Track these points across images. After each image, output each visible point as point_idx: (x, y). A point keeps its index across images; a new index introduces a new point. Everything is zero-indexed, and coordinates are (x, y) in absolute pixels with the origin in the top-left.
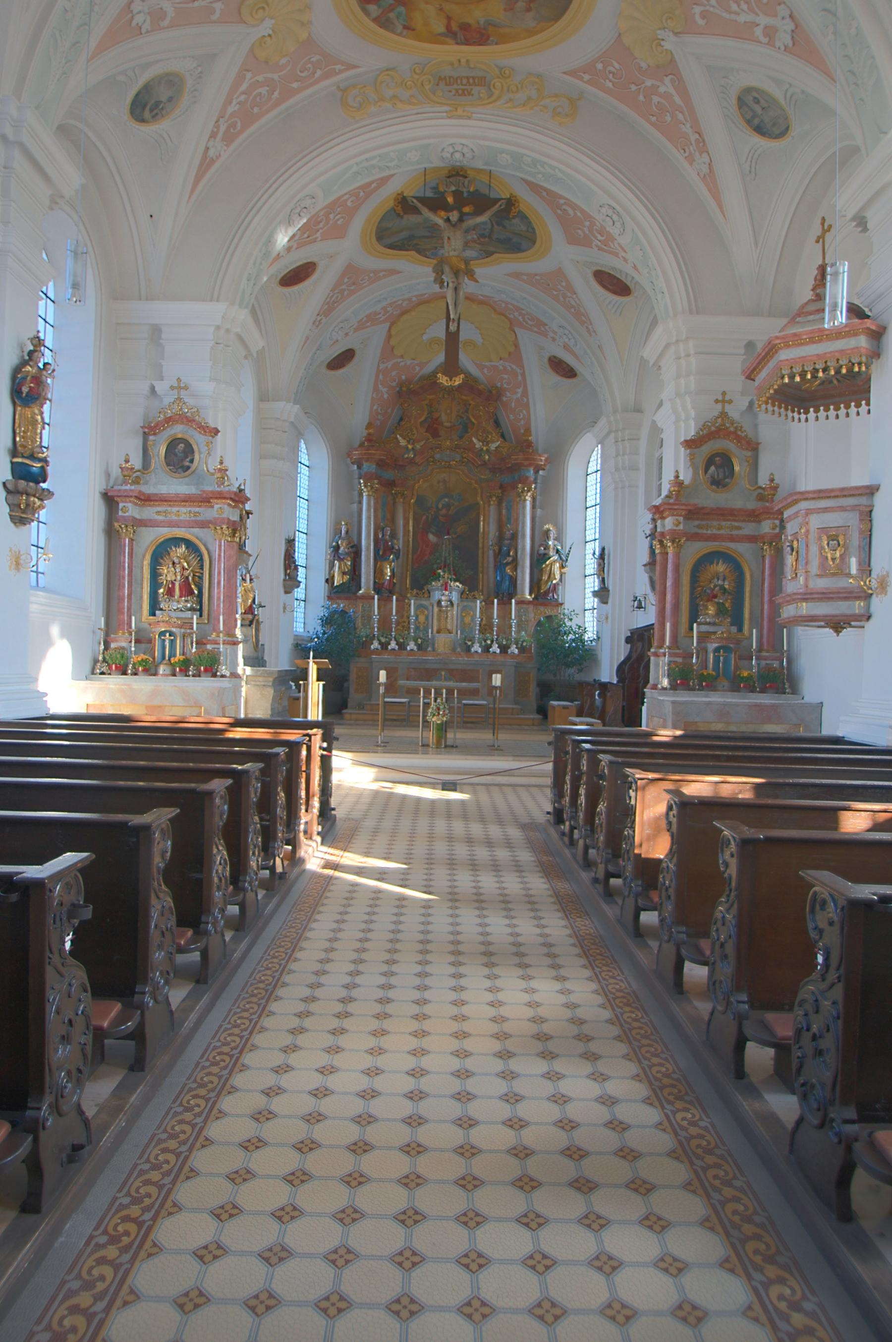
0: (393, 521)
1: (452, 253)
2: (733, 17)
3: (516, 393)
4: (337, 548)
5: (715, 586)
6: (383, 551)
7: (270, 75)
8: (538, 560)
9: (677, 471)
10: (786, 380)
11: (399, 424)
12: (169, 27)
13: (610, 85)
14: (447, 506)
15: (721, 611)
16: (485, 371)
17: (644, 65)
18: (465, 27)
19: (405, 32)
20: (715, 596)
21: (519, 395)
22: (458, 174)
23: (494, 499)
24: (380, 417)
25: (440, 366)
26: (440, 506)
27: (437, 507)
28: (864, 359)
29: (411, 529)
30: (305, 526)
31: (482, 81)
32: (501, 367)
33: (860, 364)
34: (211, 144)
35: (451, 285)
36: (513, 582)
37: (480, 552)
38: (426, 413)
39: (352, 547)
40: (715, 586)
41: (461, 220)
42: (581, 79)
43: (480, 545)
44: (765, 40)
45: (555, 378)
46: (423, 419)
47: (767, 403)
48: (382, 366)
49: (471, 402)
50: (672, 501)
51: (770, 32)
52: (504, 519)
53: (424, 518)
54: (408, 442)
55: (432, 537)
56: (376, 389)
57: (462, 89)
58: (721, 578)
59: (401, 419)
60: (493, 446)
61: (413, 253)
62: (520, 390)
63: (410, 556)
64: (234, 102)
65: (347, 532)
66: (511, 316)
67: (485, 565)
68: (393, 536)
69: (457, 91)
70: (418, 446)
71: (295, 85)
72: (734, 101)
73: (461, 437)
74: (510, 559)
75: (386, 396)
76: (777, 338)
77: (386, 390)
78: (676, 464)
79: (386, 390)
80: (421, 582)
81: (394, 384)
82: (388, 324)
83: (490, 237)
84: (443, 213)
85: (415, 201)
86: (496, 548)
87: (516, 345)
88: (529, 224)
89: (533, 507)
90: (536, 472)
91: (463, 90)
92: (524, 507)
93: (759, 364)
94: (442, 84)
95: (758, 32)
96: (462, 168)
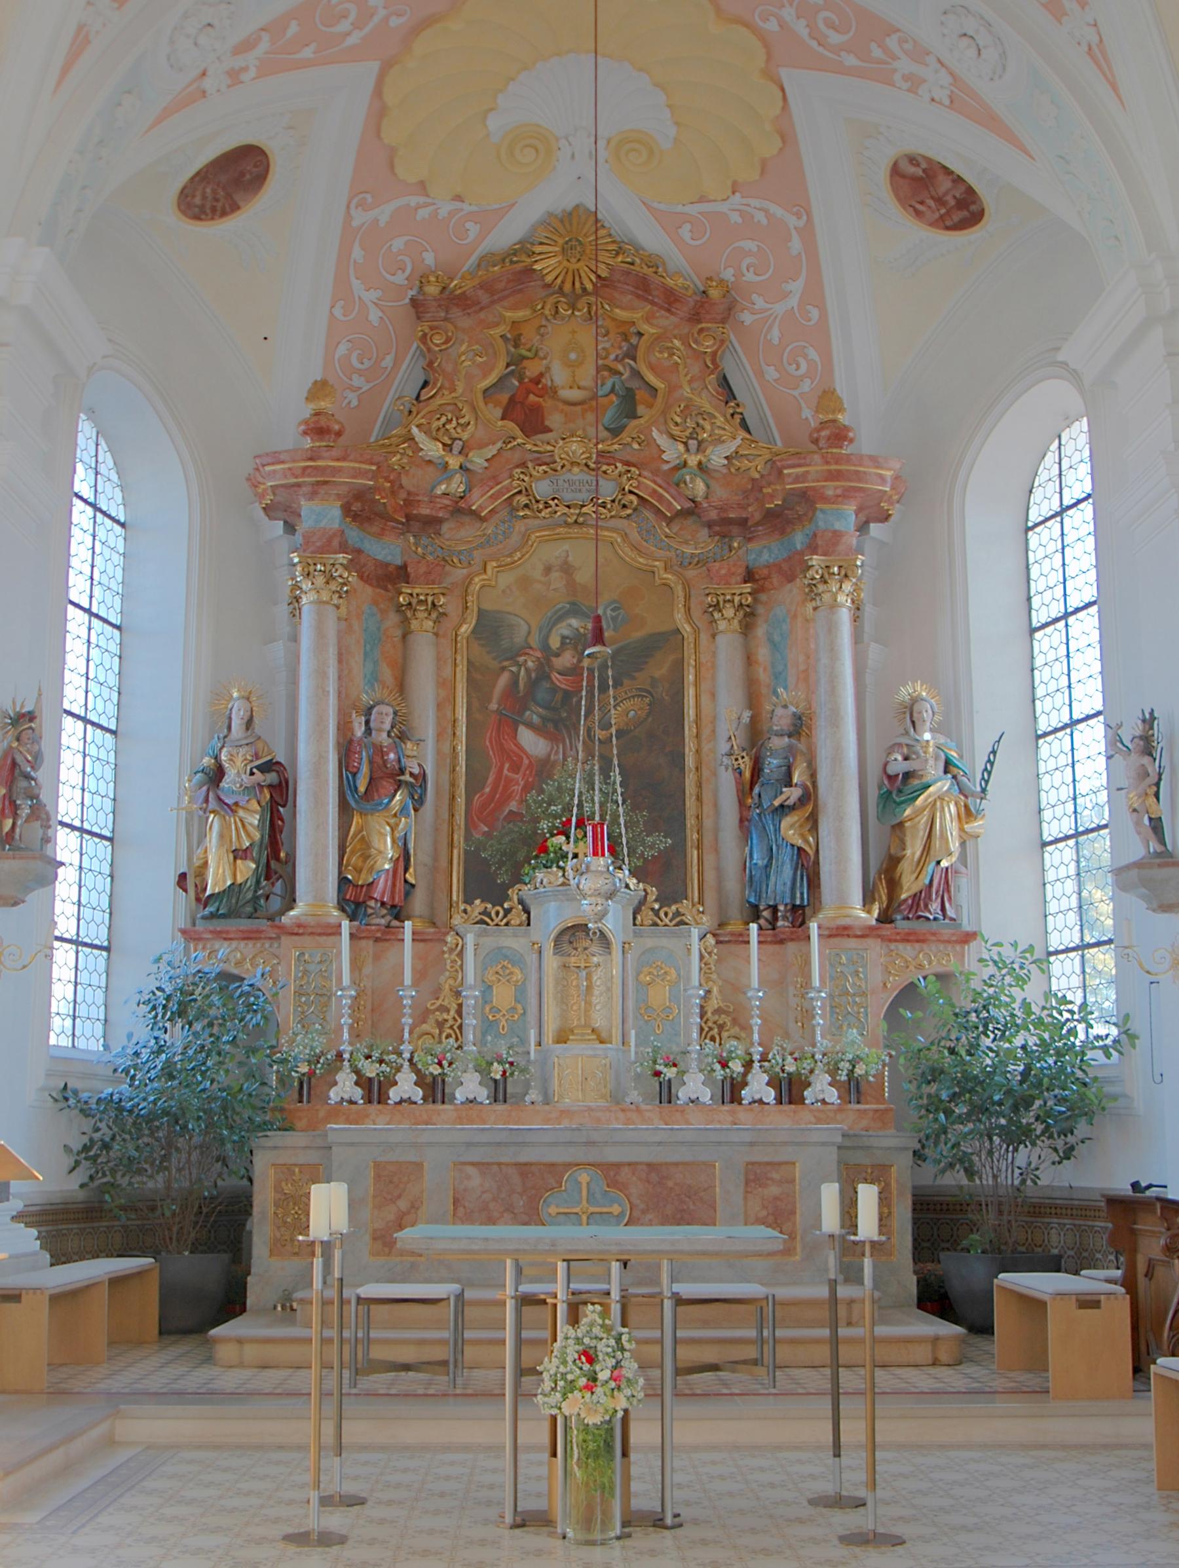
3: (786, 295)
4: (217, 774)
6: (371, 777)
16: (685, 232)
21: (793, 302)
23: (729, 612)
24: (357, 381)
26: (555, 642)
27: (546, 647)
29: (462, 714)
30: (112, 710)
32: (735, 218)
38: (502, 364)
39: (266, 768)
43: (690, 762)
45: (916, 235)
48: (360, 218)
49: (645, 328)
52: (763, 676)
53: (503, 680)
55: (531, 742)
60: (717, 457)
62: (796, 287)
63: (461, 801)
65: (249, 724)
66: (772, 26)
67: (708, 823)
68: (401, 733)
70: (478, 460)
73: (615, 432)
77: (373, 295)
79: (373, 295)
80: (494, 879)
81: (400, 278)
82: (375, 66)
86: (746, 765)
87: (786, 136)
89: (857, 638)
90: (863, 528)
92: (832, 629)
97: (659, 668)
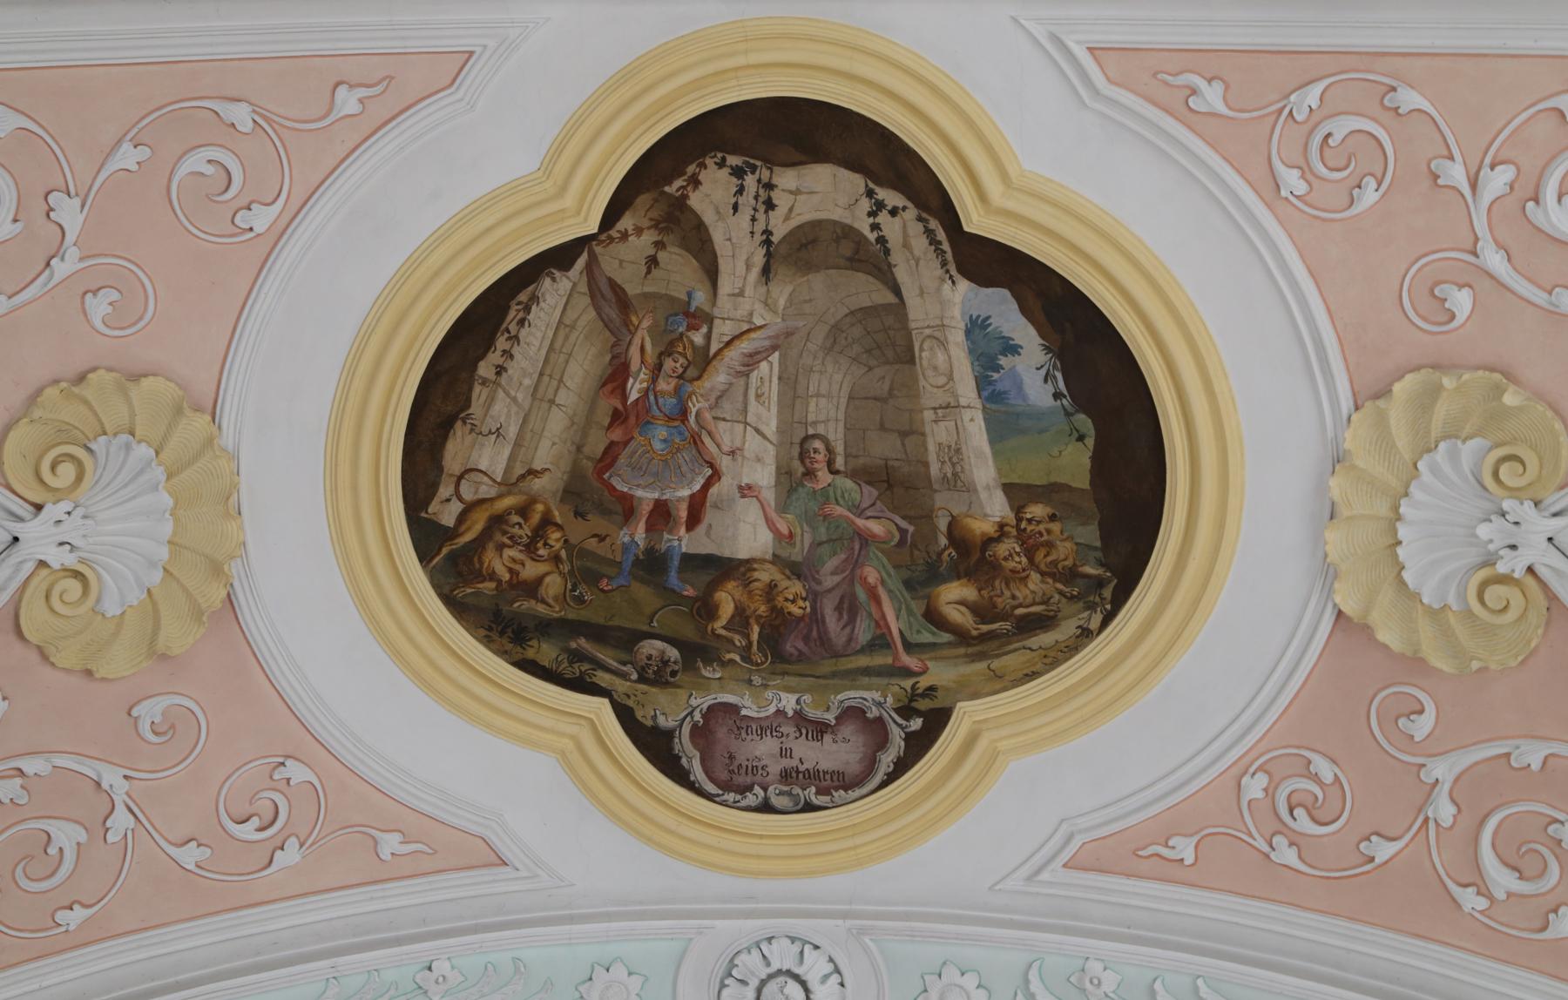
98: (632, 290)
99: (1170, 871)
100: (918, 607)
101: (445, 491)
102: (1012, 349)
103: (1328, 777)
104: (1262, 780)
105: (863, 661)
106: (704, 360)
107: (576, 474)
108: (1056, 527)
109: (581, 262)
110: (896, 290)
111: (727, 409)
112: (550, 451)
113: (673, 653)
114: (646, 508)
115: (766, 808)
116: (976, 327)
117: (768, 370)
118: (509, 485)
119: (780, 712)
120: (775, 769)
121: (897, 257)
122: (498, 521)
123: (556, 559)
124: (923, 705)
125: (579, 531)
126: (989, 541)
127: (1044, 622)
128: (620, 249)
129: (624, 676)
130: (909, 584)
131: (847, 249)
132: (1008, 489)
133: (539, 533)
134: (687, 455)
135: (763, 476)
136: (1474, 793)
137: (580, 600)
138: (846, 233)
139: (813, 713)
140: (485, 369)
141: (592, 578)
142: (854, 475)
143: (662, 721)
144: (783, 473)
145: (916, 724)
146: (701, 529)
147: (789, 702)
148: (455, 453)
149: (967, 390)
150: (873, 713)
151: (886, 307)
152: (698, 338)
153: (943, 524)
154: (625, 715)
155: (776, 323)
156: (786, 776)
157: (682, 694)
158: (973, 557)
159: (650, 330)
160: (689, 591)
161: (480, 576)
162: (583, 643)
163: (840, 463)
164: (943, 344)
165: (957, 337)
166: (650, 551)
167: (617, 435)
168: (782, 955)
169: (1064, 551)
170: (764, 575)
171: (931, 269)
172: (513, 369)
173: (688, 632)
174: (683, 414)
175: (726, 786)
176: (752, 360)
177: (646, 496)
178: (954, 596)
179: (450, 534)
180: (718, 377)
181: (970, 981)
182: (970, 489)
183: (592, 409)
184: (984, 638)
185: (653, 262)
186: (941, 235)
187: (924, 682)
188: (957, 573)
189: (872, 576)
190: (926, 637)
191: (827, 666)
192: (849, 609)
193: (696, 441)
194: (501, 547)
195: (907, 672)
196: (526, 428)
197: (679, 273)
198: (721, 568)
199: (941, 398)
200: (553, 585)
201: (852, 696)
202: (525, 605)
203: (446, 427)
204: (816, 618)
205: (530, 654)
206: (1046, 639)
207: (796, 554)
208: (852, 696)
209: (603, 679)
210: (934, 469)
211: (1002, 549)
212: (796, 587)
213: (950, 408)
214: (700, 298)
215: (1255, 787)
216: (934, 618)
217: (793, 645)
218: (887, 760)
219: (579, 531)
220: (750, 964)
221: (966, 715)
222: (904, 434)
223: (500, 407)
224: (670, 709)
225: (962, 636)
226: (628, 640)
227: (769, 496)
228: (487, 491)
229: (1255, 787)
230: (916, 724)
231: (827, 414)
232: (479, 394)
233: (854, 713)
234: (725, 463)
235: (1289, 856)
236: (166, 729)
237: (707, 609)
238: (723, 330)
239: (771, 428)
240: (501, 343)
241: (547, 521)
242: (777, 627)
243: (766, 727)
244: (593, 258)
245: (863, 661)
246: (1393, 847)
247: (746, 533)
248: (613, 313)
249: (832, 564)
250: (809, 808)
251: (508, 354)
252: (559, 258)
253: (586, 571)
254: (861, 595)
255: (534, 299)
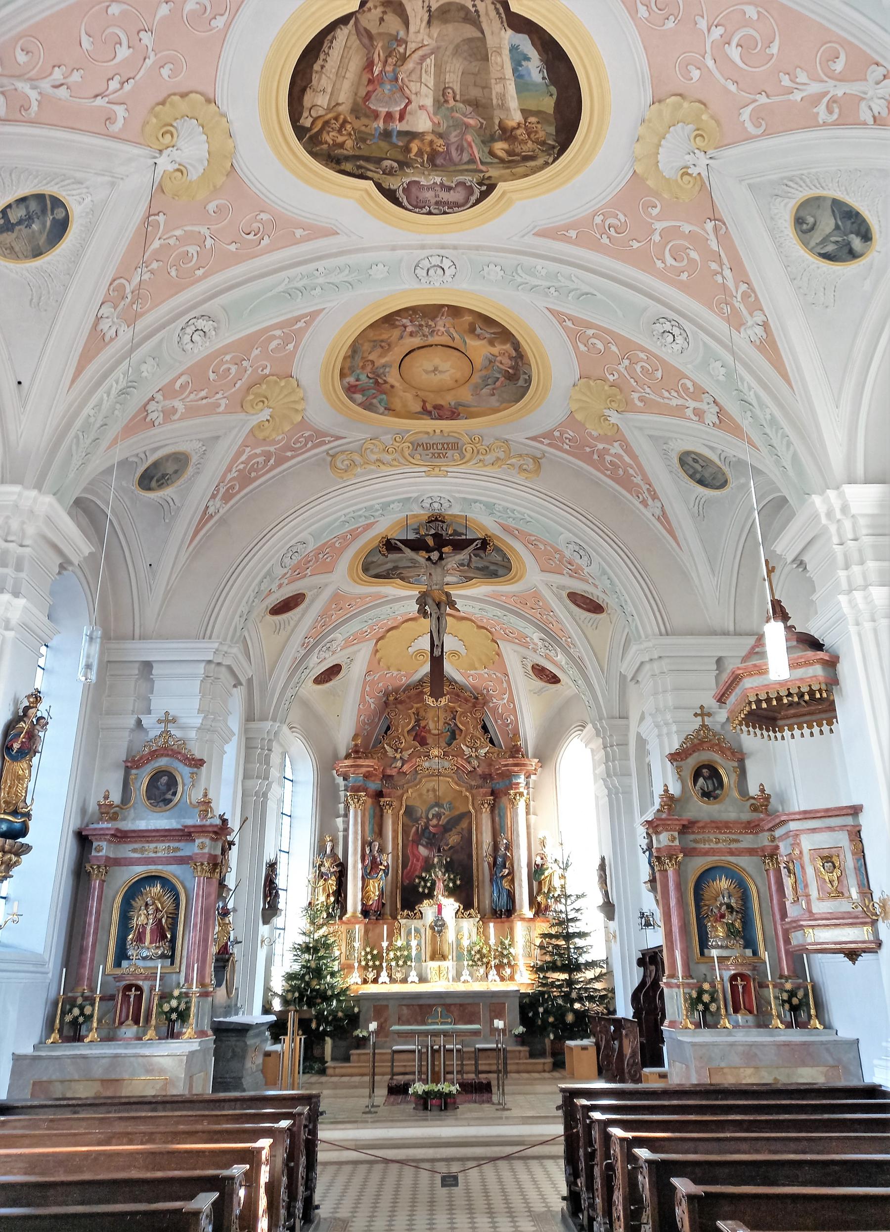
0: (380, 832)
1: (434, 587)
2: (666, 401)
5: (721, 904)
7: (267, 448)
8: (536, 871)
9: (666, 785)
10: (754, 707)
11: (386, 733)
12: (179, 419)
13: (568, 447)
14: (438, 816)
15: (731, 932)
17: (595, 433)
18: (438, 407)
19: (386, 412)
20: (723, 916)
22: (436, 520)
23: (486, 805)
24: (366, 727)
25: (426, 675)
26: (430, 816)
27: (427, 818)
28: (824, 687)
31: (455, 446)
33: (820, 691)
34: (210, 504)
35: (434, 615)
36: (511, 896)
37: (474, 863)
40: (721, 904)
41: (441, 558)
42: (542, 443)
44: (697, 418)
46: (410, 727)
47: (741, 724)
50: (664, 816)
51: (699, 414)
52: (498, 827)
53: (414, 829)
54: (396, 751)
55: (423, 851)
56: (363, 700)
57: (437, 452)
58: (726, 895)
59: (388, 728)
61: (399, 581)
64: (234, 470)
67: (480, 878)
69: (433, 454)
71: (289, 454)
72: (678, 465)
73: (449, 745)
74: (507, 871)
75: (373, 706)
76: (739, 668)
77: (372, 700)
78: (665, 779)
79: (372, 700)
80: (411, 897)
81: (381, 694)
83: (468, 565)
84: (423, 553)
85: (398, 543)
86: (491, 860)
88: (504, 556)
91: (439, 454)
93: (727, 689)
94: (420, 449)
95: (689, 412)
96: (440, 515)
97: (464, 824)
98: (374, 31)
99: (567, 240)
100: (486, 150)
101: (305, 114)
102: (527, 59)
103: (623, 221)
104: (601, 217)
105: (466, 167)
106: (404, 59)
107: (355, 103)
108: (539, 126)
109: (352, 22)
110: (483, 32)
111: (414, 77)
112: (345, 97)
113: (395, 165)
114: (383, 115)
115: (430, 213)
116: (514, 49)
117: (430, 62)
118: (329, 110)
119: (435, 183)
120: (433, 201)
121: (483, 19)
122: (327, 123)
123: (350, 134)
124: (487, 182)
125: (357, 124)
126: (514, 129)
127: (532, 158)
128: (369, 15)
129: (378, 173)
130: (483, 142)
131: (462, 14)
132: (523, 111)
133: (343, 126)
134: (398, 95)
135: (429, 102)
136: (668, 234)
137: (360, 148)
138: (463, 8)
139: (447, 183)
140: (316, 67)
141: (364, 140)
142: (464, 102)
143: (392, 187)
144: (436, 102)
145: (484, 188)
146: (404, 121)
147: (438, 180)
148: (308, 99)
149: (509, 72)
150: (469, 184)
151: (478, 38)
152: (401, 50)
153: (497, 122)
154: (379, 186)
155: (433, 44)
156: (437, 203)
157: (399, 178)
158: (507, 134)
159: (382, 48)
160: (400, 144)
161: (321, 143)
162: (361, 163)
163: (458, 98)
164: (500, 54)
165: (506, 52)
166: (385, 130)
167: (370, 88)
168: (436, 261)
169: (541, 135)
170: (429, 138)
171: (497, 23)
172: (327, 66)
173: (401, 157)
174: (396, 79)
175: (416, 207)
176: (423, 58)
177: (383, 110)
178: (500, 147)
179: (309, 130)
180: (410, 65)
181: (498, 268)
182: (508, 110)
183: (360, 77)
184: (510, 162)
185: (382, 20)
186: (501, 10)
187: (487, 175)
188: (501, 139)
189: (469, 138)
190: (489, 160)
191: (452, 169)
192: (461, 149)
193: (401, 89)
194: (328, 133)
195: (482, 172)
196: (335, 87)
197: (393, 23)
198: (412, 135)
199: (499, 75)
200: (349, 144)
201: (461, 178)
202: (339, 151)
203: (303, 90)
204: (448, 152)
205: (343, 167)
206: (532, 164)
207: (441, 130)
208: (461, 178)
209: (369, 174)
210: (495, 102)
211: (519, 132)
212: (441, 142)
213: (502, 79)
214: (402, 34)
215: (598, 220)
216: (492, 153)
217: (439, 161)
218: (473, 199)
219: (357, 124)
220: (426, 264)
221: (501, 187)
222: (483, 88)
223: (324, 81)
224: (394, 183)
225: (502, 161)
226: (378, 161)
227: (431, 110)
228: (321, 112)
229: (598, 220)
230: (484, 188)
231: (453, 79)
232: (315, 77)
233: (462, 184)
234: (413, 97)
235: (607, 241)
236: (219, 210)
237: (407, 150)
238: (412, 46)
239: (431, 84)
240: (322, 56)
241: (345, 121)
242: (433, 157)
243: (429, 188)
244: (356, 19)
245: (466, 167)
246: (639, 244)
247: (422, 123)
248: (366, 40)
249: (454, 134)
250: (445, 213)
251: (325, 60)
252: (344, 20)
253: (362, 138)
254: (465, 145)
255: (334, 38)
